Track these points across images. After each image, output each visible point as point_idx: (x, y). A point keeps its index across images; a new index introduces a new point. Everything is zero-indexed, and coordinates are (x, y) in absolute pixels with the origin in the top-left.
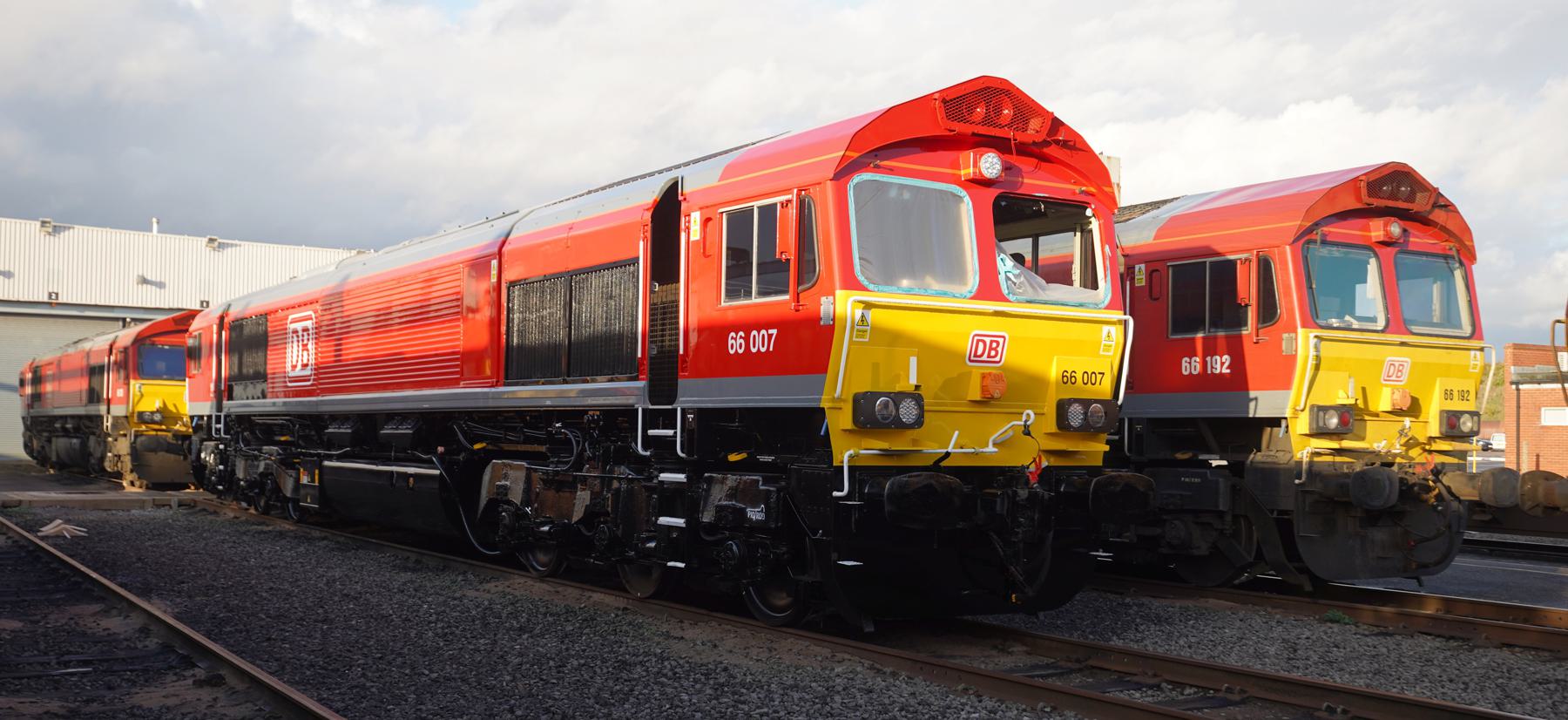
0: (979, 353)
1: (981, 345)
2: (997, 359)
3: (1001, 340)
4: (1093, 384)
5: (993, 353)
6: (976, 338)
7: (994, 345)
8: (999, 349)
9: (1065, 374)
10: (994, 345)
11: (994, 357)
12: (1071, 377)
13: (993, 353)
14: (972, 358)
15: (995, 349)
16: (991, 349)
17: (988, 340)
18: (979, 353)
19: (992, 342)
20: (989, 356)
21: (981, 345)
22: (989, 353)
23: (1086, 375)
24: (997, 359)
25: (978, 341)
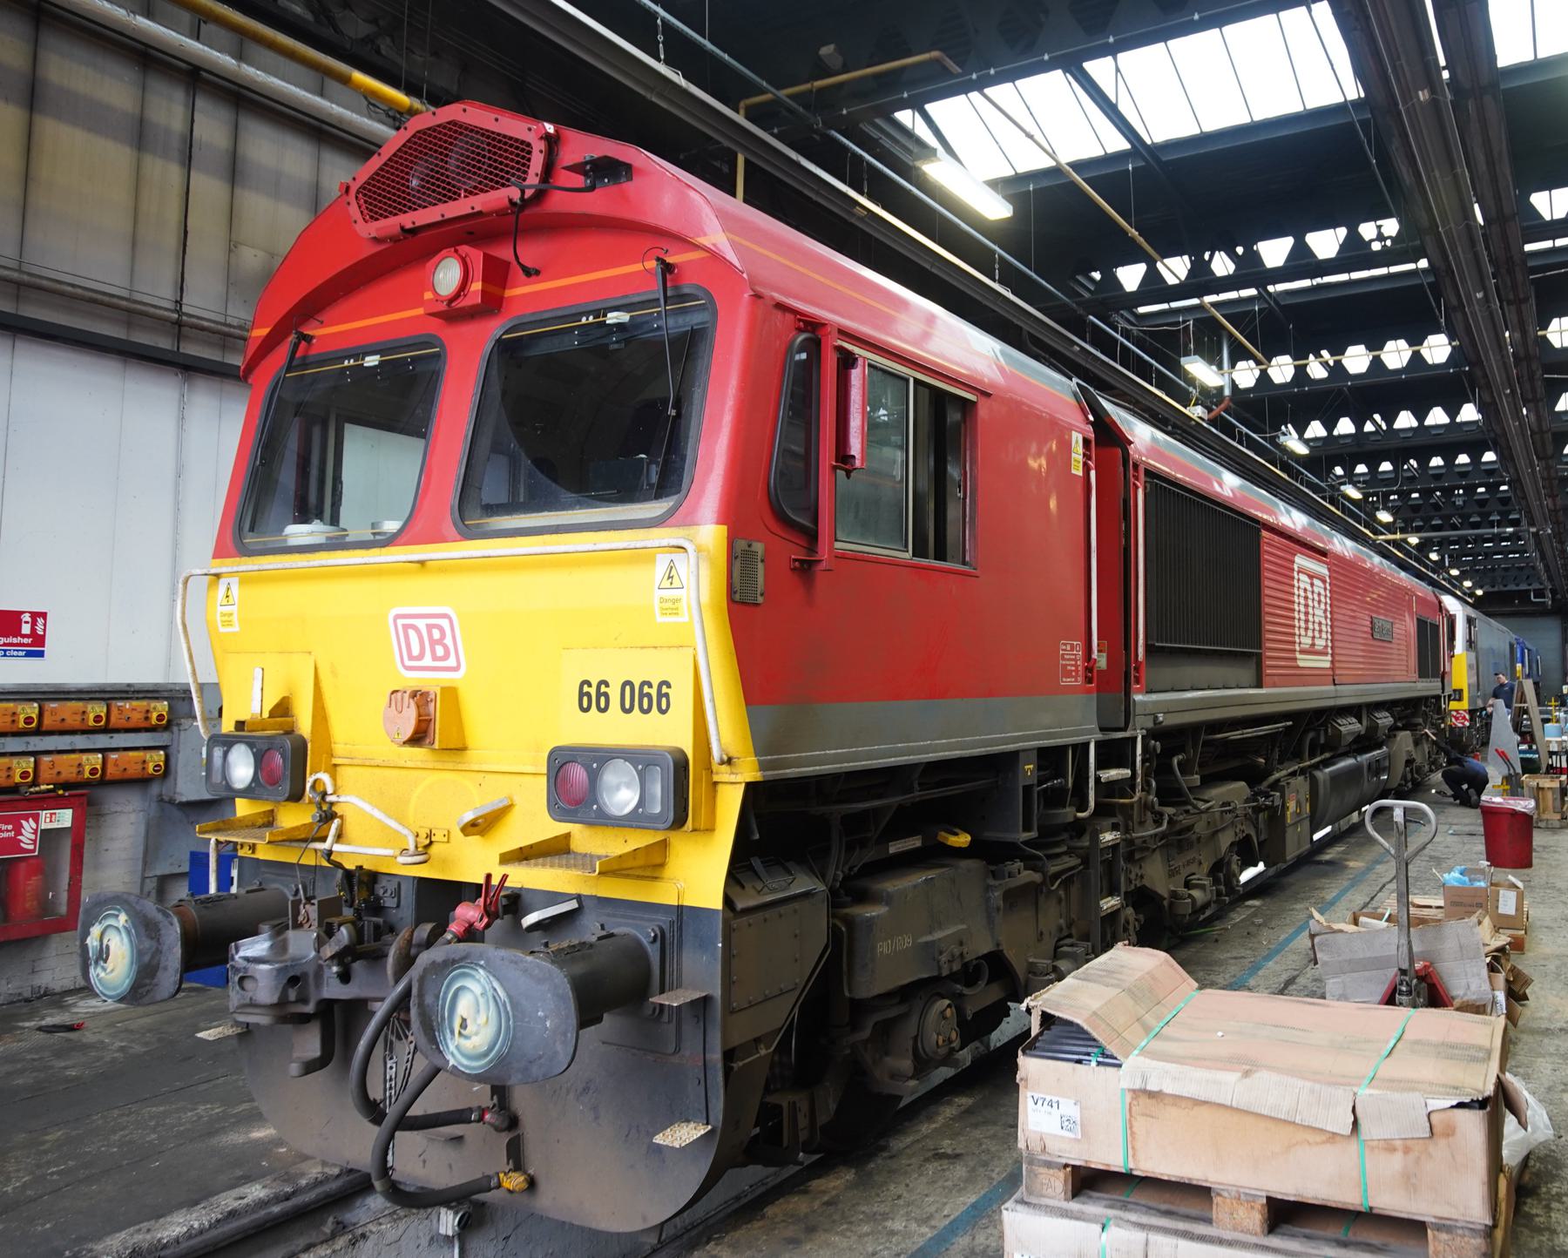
0: (416, 651)
1: (412, 633)
2: (451, 662)
3: (444, 623)
4: (604, 710)
5: (440, 651)
6: (400, 622)
7: (436, 634)
8: (448, 641)
9: (586, 689)
10: (436, 634)
11: (446, 657)
12: (599, 694)
13: (440, 651)
14: (408, 663)
15: (441, 642)
16: (433, 643)
17: (421, 624)
18: (416, 651)
19: (430, 627)
20: (435, 658)
21: (412, 633)
22: (433, 651)
23: (628, 688)
24: (451, 662)
25: (406, 627)
